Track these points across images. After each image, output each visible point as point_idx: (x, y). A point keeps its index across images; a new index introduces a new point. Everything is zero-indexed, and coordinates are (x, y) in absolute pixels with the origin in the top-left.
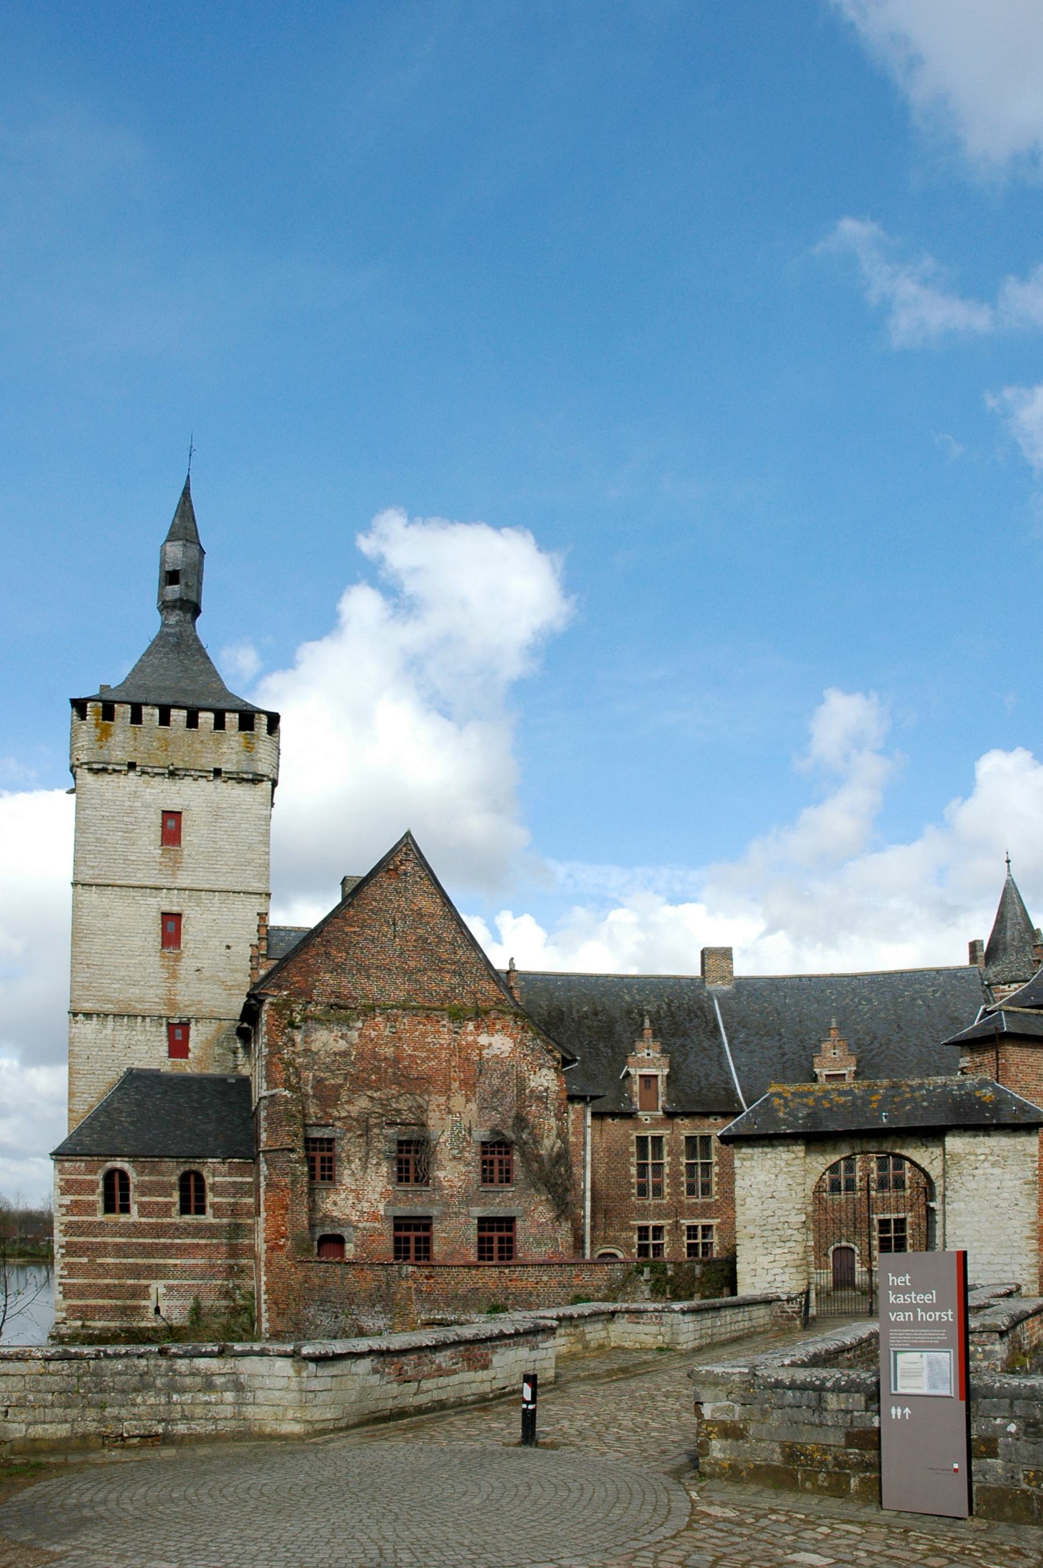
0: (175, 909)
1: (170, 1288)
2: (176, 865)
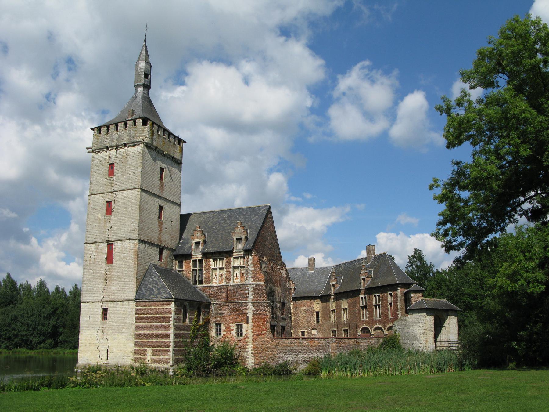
0: (162, 205)
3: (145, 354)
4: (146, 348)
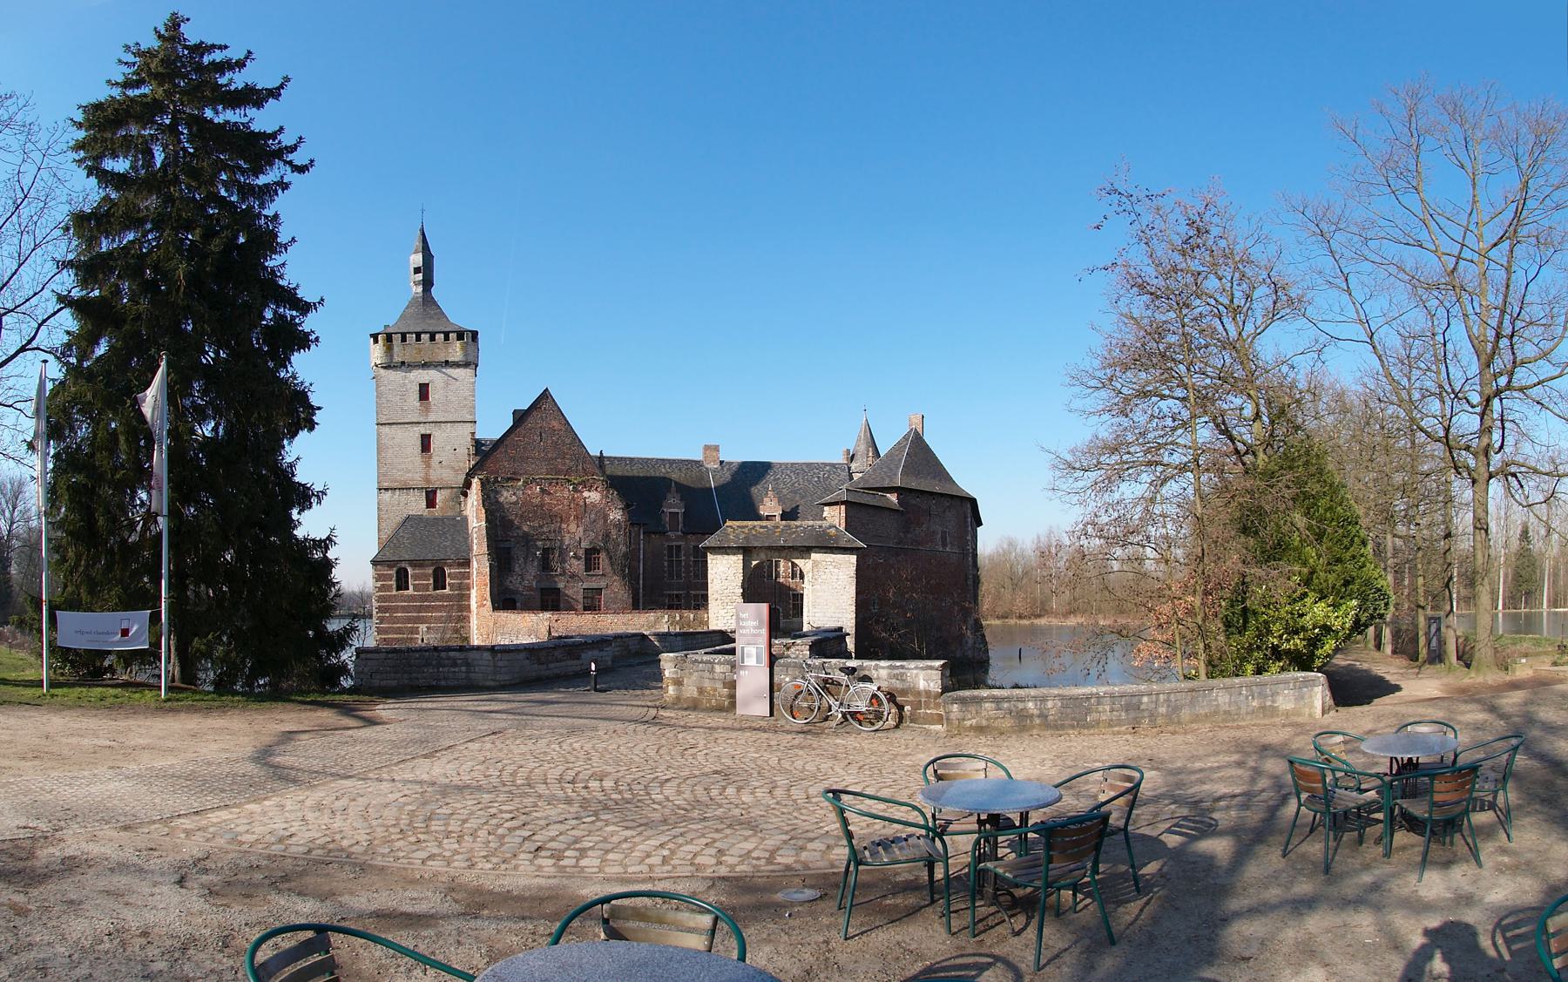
0: (428, 432)
1: (428, 628)
2: (427, 410)
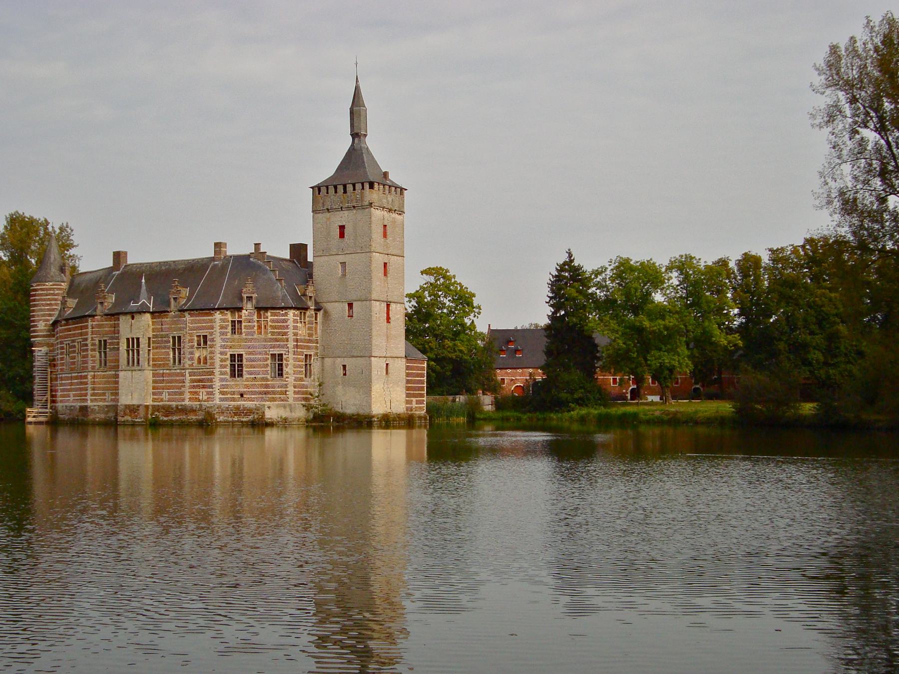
3: (412, 404)
4: (412, 399)
